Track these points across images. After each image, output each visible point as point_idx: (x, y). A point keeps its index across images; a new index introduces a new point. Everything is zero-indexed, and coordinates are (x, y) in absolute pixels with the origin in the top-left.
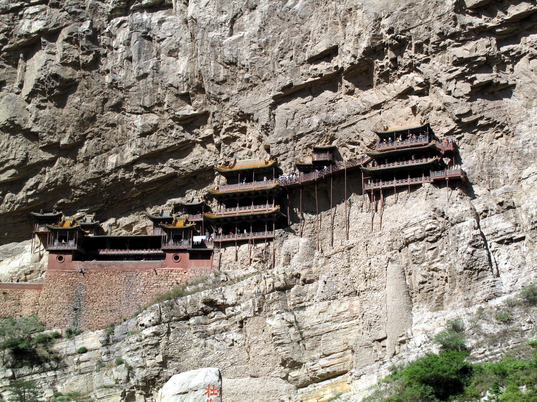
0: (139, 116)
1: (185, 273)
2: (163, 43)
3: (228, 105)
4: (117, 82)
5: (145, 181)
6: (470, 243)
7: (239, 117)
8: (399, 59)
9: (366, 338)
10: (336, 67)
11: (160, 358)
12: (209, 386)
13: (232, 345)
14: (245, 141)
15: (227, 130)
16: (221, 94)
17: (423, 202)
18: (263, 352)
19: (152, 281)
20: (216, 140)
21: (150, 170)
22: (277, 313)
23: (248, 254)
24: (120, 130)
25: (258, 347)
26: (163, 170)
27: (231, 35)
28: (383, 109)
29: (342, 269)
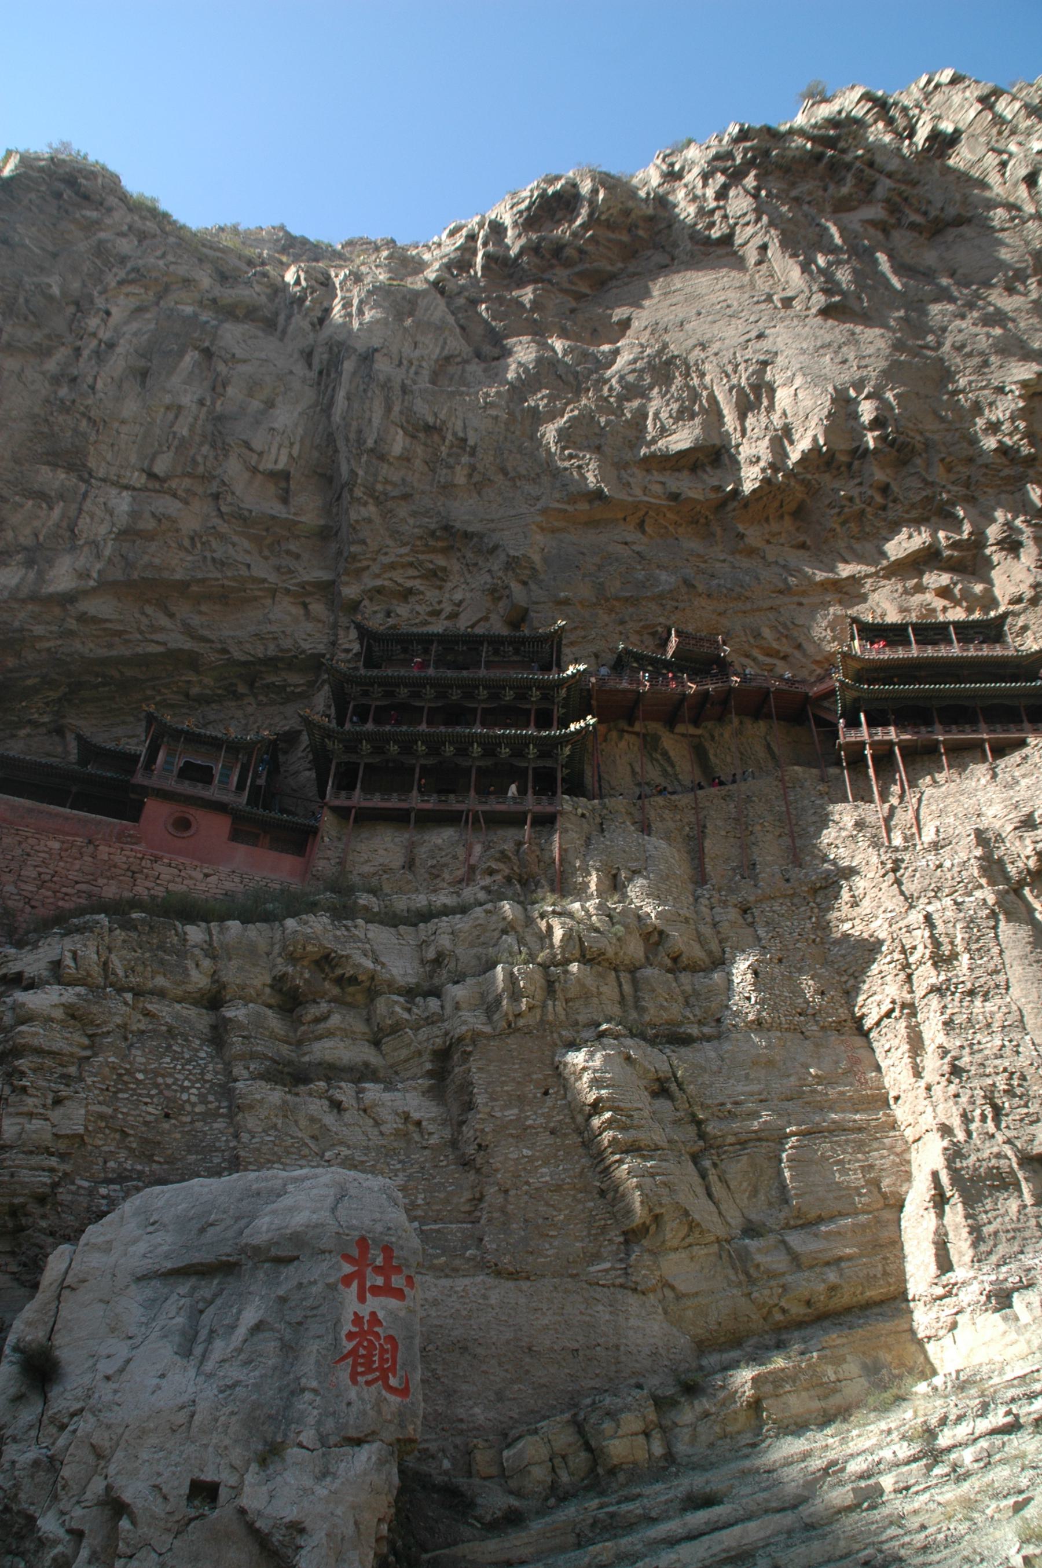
0: (124, 493)
1: (207, 876)
2: (242, 368)
3: (403, 511)
4: (90, 402)
5: (92, 655)
7: (431, 543)
8: (895, 488)
10: (719, 489)
12: (363, 1243)
13: (397, 1133)
14: (440, 602)
15: (392, 566)
16: (387, 482)
18: (545, 1175)
19: (73, 875)
20: (350, 591)
21: (120, 627)
22: (602, 1035)
23: (461, 852)
24: (57, 512)
25: (526, 1152)
28: (846, 593)
29: (798, 945)
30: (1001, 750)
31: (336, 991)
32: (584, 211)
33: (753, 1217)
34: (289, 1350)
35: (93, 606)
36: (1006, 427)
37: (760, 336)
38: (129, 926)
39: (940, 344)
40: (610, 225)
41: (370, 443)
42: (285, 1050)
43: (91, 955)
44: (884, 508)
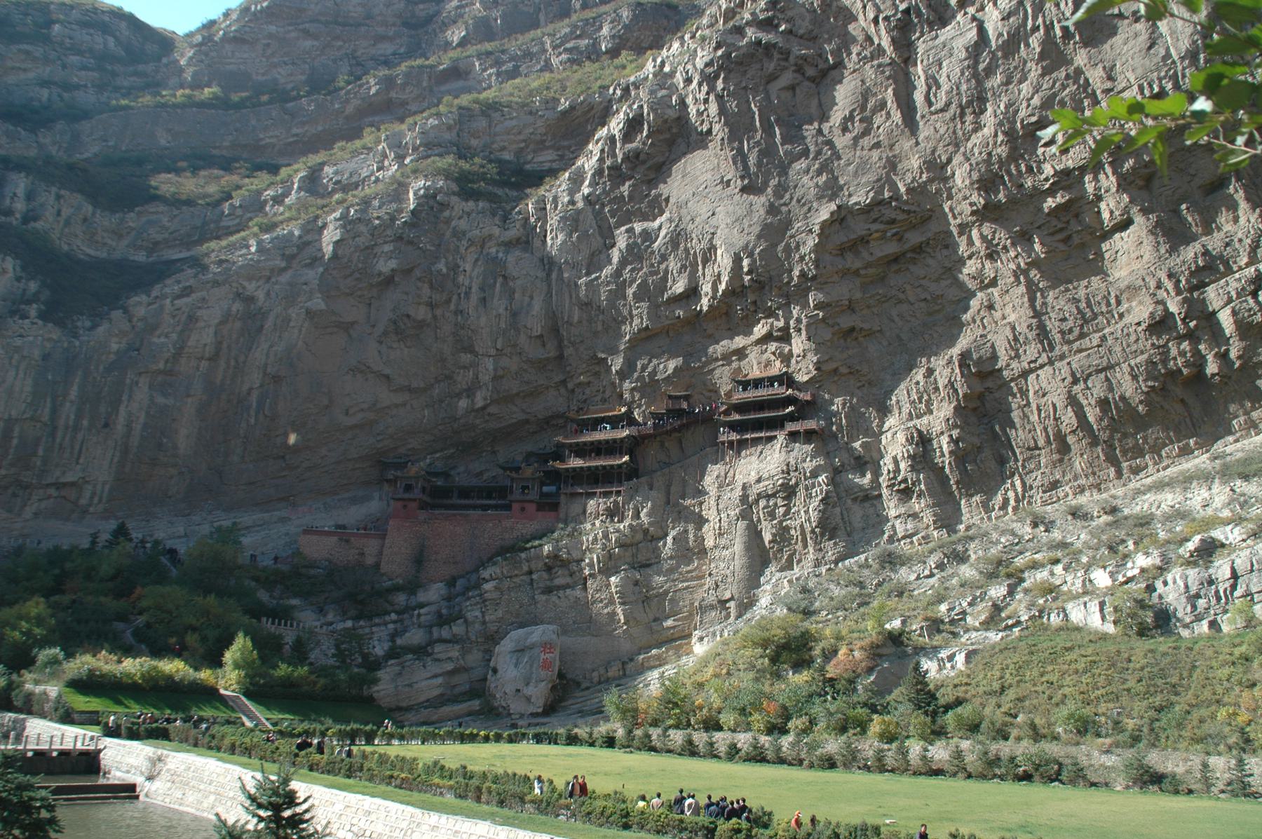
2: (519, 282)
6: (821, 500)
8: (758, 303)
9: (712, 599)
11: (500, 613)
17: (777, 455)
20: (570, 386)
26: (514, 416)
27: (588, 274)
30: (771, 439)
31: (559, 563)
32: (646, 126)
33: (657, 616)
34: (531, 666)
35: (493, 409)
36: (807, 258)
37: (713, 214)
38: (506, 559)
39: (791, 199)
40: (659, 131)
41: (566, 318)
42: (548, 583)
43: (498, 571)
44: (755, 311)
